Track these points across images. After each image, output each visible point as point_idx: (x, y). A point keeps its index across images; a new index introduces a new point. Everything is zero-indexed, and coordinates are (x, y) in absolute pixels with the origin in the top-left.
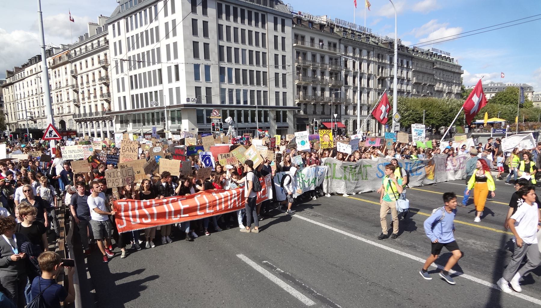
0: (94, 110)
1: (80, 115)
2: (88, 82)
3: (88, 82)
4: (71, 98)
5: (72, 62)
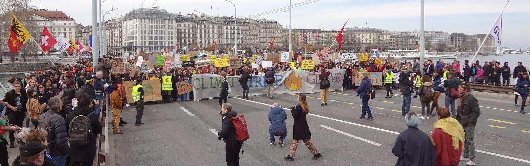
0: (117, 46)
1: (113, 47)
2: (116, 37)
3: (116, 37)
4: (111, 41)
5: (111, 29)
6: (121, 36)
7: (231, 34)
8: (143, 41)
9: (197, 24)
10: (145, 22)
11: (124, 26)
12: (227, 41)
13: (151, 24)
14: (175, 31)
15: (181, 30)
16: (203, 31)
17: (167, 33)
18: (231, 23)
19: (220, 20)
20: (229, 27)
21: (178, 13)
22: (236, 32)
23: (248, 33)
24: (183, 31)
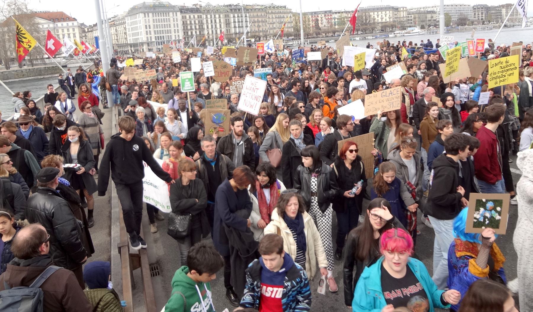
6: (126, 33)
7: (239, 22)
8: (149, 36)
9: (202, 15)
10: (148, 17)
11: (128, 22)
12: (235, 30)
13: (155, 18)
14: (180, 23)
15: (186, 21)
16: (209, 21)
17: (172, 26)
18: (237, 10)
19: (226, 8)
20: (236, 15)
21: (182, 4)
22: (244, 20)
23: (256, 19)
24: (188, 22)
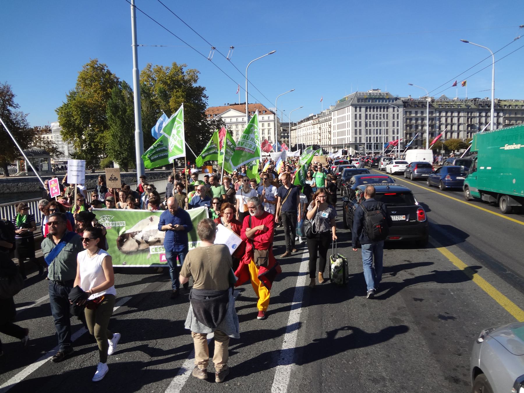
8: (358, 136)
